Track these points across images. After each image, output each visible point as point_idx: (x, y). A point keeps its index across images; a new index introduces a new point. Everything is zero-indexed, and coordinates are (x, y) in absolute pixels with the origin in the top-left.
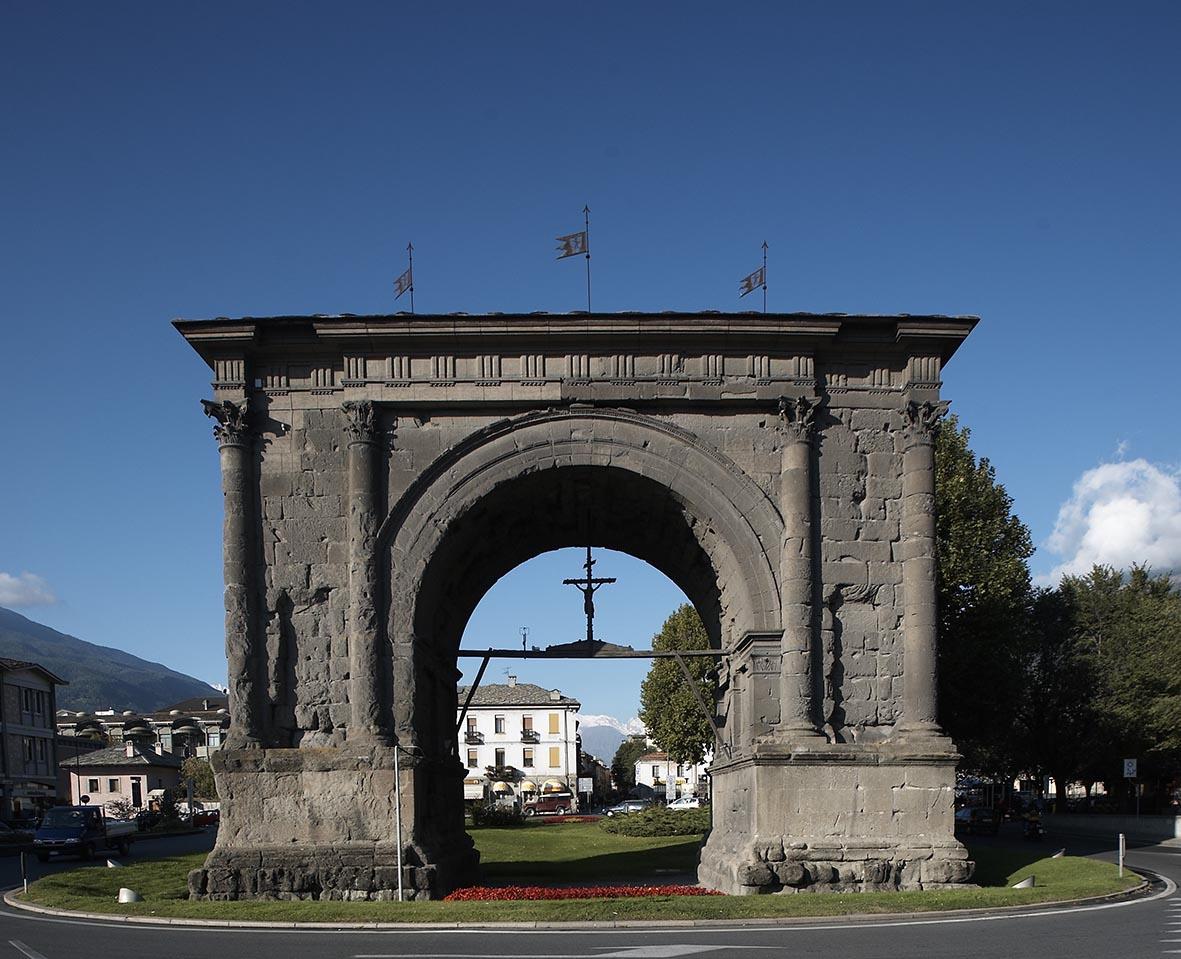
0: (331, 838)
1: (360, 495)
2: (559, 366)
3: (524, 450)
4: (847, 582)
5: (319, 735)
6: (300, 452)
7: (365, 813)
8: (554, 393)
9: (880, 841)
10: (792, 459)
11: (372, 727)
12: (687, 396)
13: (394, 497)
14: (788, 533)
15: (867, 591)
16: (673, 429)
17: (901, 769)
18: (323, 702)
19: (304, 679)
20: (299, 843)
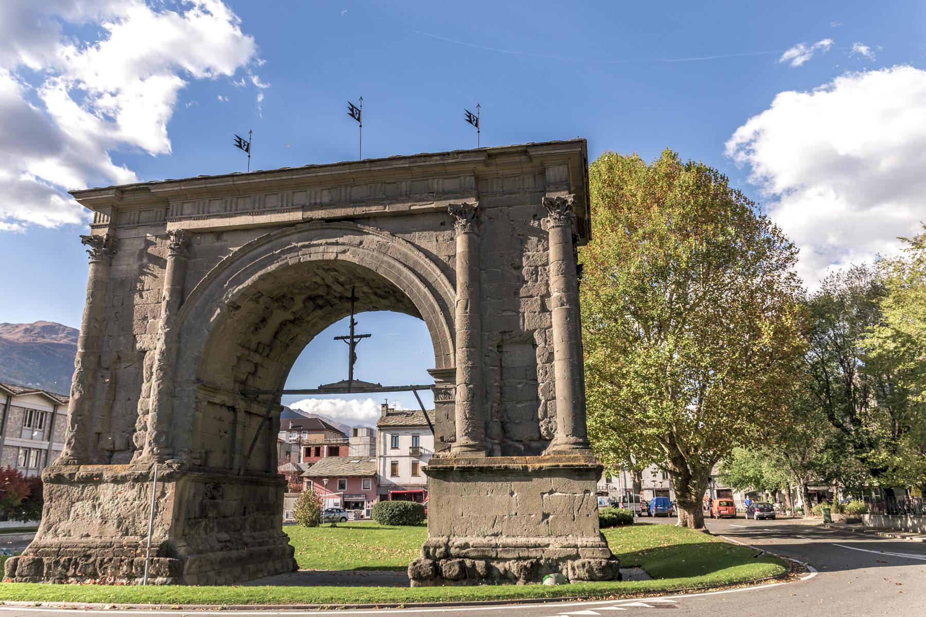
6: (139, 263)
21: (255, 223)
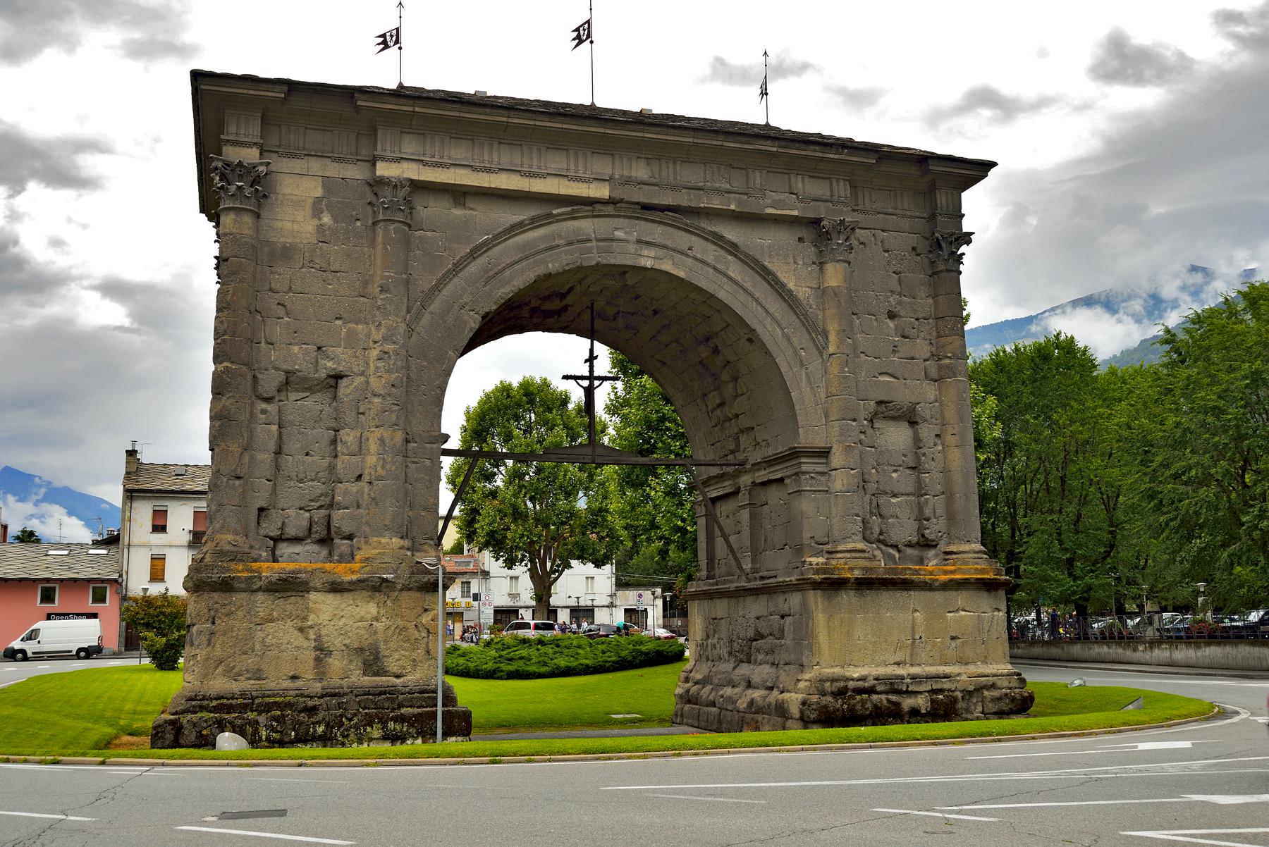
8: (602, 191)
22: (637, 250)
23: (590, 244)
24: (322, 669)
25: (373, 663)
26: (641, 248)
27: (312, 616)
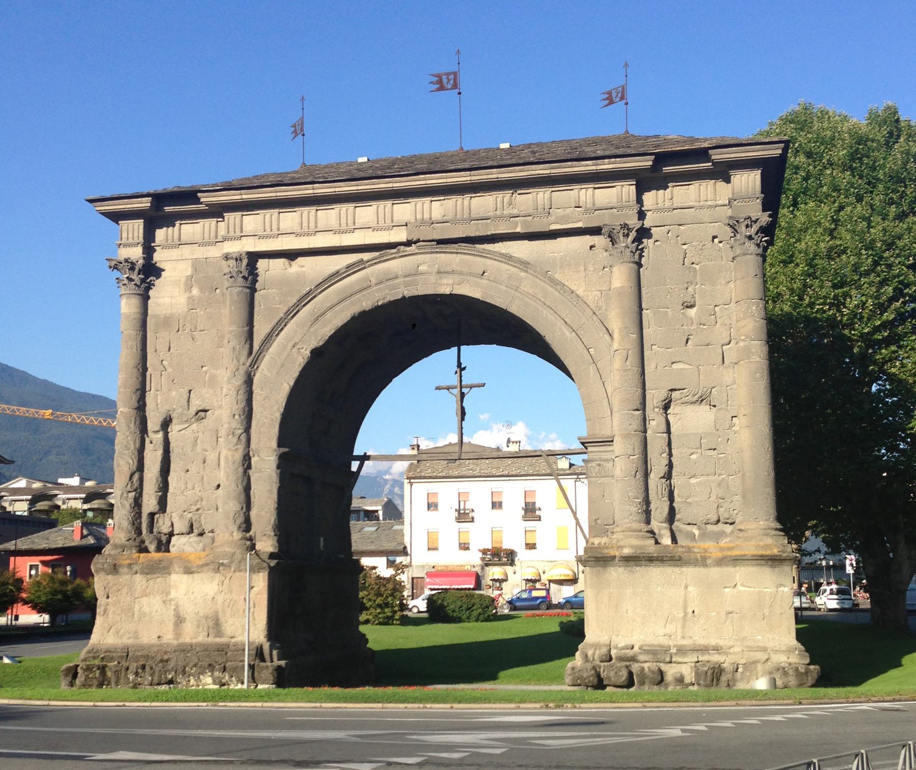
0: (192, 634)
1: (232, 331)
2: (405, 210)
3: (377, 284)
4: (678, 387)
5: (193, 538)
7: (224, 612)
8: (400, 236)
9: (713, 641)
10: (620, 277)
11: (235, 534)
12: (518, 230)
13: (261, 330)
14: (616, 345)
15: (699, 394)
16: (508, 258)
17: (730, 569)
18: (198, 510)
19: (182, 489)
20: (165, 640)
21: (342, 245)
22: (437, 280)
23: (397, 281)
24: (179, 632)
25: (216, 625)
26: (441, 278)
27: (173, 592)
